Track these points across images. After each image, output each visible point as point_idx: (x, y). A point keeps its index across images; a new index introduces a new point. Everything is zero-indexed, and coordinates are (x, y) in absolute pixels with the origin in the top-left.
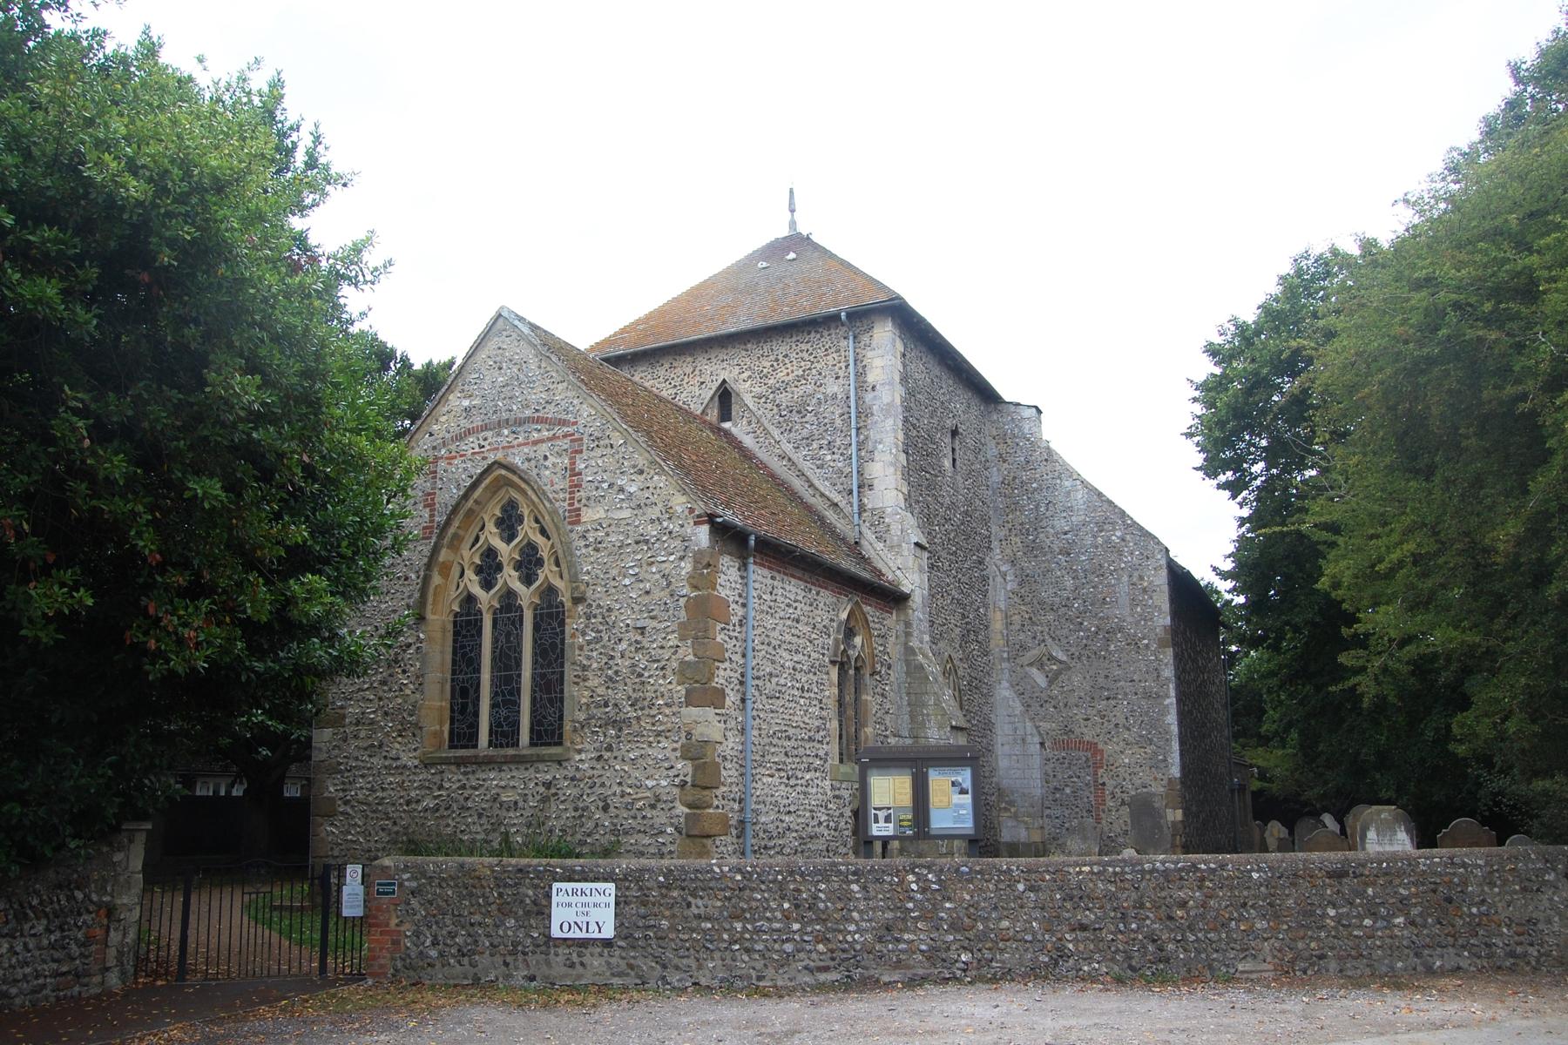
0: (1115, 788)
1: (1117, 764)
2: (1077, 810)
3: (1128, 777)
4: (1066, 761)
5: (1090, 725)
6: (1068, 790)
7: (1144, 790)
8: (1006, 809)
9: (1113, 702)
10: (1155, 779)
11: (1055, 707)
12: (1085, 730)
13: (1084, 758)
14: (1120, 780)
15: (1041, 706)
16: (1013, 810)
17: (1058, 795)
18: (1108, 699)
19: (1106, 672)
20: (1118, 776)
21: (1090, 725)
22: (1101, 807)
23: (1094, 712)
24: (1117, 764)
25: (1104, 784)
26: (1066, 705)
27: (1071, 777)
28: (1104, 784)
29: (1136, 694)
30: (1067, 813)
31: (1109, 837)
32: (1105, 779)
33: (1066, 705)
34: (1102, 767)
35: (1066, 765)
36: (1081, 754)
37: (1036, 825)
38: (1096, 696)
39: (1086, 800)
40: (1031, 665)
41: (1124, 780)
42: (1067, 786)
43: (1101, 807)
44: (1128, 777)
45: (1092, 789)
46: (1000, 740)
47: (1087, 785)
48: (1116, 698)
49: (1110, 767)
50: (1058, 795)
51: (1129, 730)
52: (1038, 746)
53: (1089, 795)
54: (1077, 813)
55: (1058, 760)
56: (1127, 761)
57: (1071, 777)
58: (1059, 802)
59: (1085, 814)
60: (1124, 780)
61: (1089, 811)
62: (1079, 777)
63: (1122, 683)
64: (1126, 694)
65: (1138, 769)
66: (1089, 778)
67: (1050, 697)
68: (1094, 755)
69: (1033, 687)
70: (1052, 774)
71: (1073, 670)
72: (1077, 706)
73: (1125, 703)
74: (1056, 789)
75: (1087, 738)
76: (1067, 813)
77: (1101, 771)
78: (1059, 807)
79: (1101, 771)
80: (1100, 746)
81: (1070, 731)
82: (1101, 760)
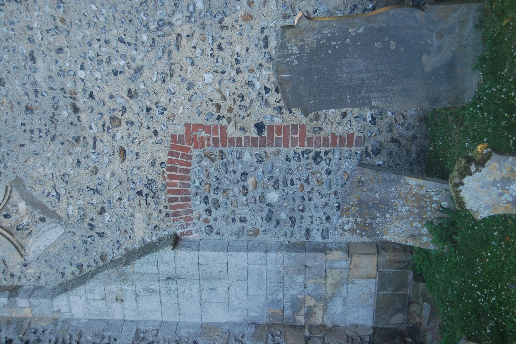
0: (267, 104)
1: (217, 98)
2: (313, 181)
3: (245, 76)
4: (212, 196)
5: (135, 148)
6: (273, 196)
7: (273, 43)
8: (309, 314)
9: (82, 101)
10: (248, 17)
11: (103, 211)
12: (145, 159)
13: (206, 162)
14: (250, 94)
15: (101, 235)
16: (310, 302)
17: (283, 216)
18: (76, 110)
19: (19, 110)
20: (242, 97)
21: (135, 148)
22: (309, 135)
23: (106, 137)
24: (217, 98)
25: (260, 127)
26: (95, 191)
27: (245, 190)
28: (260, 127)
29: (60, 50)
30: (317, 200)
31: (374, 121)
32: (250, 123)
33: (95, 191)
34: (223, 129)
35: (220, 197)
36: (195, 167)
37: (344, 264)
38: (71, 133)
39: (293, 163)
40: (20, 249)
41: (250, 84)
42: (262, 198)
43: (309, 135)
44: (245, 76)
45: (270, 150)
46: (170, 317)
47: (260, 161)
48: (73, 96)
49: (223, 112)
50: (283, 216)
51: (139, 70)
52: (181, 253)
53: (282, 157)
54: (320, 182)
55: (209, 211)
56: (209, 77)
57: (245, 190)
58: (297, 215)
59: (323, 166)
60: (250, 84)
61: (317, 158)
62: (245, 174)
63: (39, 77)
64: (62, 73)
65: (226, 54)
66: (247, 157)
67: (82, 219)
68: (199, 144)
69: (66, 248)
70: (238, 224)
71: (21, 175)
72: (95, 171)
73: (81, 74)
74: (269, 219)
75: (163, 156)
76: (317, 200)
77: (232, 131)
78: (307, 214)
79: (232, 131)
80: (180, 130)
81: (148, 185)
82: (207, 129)
